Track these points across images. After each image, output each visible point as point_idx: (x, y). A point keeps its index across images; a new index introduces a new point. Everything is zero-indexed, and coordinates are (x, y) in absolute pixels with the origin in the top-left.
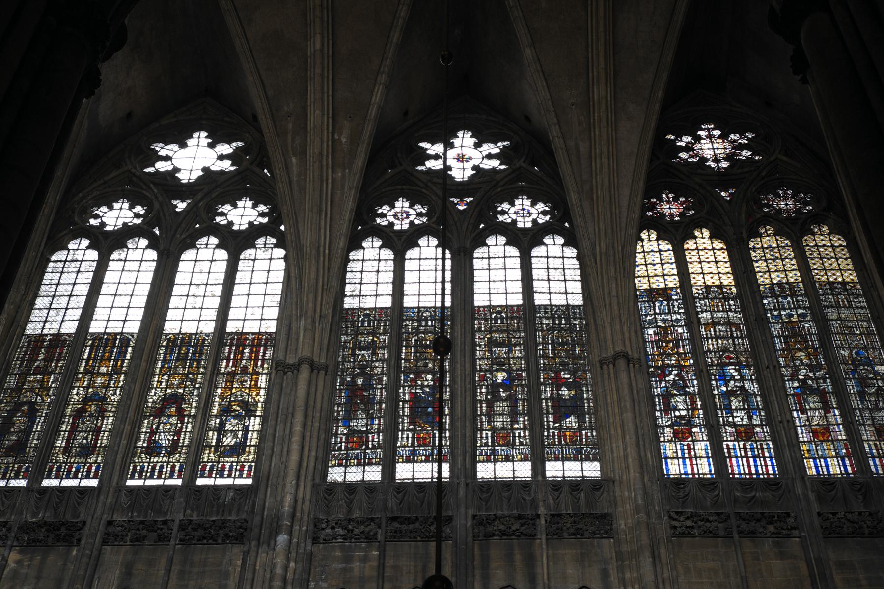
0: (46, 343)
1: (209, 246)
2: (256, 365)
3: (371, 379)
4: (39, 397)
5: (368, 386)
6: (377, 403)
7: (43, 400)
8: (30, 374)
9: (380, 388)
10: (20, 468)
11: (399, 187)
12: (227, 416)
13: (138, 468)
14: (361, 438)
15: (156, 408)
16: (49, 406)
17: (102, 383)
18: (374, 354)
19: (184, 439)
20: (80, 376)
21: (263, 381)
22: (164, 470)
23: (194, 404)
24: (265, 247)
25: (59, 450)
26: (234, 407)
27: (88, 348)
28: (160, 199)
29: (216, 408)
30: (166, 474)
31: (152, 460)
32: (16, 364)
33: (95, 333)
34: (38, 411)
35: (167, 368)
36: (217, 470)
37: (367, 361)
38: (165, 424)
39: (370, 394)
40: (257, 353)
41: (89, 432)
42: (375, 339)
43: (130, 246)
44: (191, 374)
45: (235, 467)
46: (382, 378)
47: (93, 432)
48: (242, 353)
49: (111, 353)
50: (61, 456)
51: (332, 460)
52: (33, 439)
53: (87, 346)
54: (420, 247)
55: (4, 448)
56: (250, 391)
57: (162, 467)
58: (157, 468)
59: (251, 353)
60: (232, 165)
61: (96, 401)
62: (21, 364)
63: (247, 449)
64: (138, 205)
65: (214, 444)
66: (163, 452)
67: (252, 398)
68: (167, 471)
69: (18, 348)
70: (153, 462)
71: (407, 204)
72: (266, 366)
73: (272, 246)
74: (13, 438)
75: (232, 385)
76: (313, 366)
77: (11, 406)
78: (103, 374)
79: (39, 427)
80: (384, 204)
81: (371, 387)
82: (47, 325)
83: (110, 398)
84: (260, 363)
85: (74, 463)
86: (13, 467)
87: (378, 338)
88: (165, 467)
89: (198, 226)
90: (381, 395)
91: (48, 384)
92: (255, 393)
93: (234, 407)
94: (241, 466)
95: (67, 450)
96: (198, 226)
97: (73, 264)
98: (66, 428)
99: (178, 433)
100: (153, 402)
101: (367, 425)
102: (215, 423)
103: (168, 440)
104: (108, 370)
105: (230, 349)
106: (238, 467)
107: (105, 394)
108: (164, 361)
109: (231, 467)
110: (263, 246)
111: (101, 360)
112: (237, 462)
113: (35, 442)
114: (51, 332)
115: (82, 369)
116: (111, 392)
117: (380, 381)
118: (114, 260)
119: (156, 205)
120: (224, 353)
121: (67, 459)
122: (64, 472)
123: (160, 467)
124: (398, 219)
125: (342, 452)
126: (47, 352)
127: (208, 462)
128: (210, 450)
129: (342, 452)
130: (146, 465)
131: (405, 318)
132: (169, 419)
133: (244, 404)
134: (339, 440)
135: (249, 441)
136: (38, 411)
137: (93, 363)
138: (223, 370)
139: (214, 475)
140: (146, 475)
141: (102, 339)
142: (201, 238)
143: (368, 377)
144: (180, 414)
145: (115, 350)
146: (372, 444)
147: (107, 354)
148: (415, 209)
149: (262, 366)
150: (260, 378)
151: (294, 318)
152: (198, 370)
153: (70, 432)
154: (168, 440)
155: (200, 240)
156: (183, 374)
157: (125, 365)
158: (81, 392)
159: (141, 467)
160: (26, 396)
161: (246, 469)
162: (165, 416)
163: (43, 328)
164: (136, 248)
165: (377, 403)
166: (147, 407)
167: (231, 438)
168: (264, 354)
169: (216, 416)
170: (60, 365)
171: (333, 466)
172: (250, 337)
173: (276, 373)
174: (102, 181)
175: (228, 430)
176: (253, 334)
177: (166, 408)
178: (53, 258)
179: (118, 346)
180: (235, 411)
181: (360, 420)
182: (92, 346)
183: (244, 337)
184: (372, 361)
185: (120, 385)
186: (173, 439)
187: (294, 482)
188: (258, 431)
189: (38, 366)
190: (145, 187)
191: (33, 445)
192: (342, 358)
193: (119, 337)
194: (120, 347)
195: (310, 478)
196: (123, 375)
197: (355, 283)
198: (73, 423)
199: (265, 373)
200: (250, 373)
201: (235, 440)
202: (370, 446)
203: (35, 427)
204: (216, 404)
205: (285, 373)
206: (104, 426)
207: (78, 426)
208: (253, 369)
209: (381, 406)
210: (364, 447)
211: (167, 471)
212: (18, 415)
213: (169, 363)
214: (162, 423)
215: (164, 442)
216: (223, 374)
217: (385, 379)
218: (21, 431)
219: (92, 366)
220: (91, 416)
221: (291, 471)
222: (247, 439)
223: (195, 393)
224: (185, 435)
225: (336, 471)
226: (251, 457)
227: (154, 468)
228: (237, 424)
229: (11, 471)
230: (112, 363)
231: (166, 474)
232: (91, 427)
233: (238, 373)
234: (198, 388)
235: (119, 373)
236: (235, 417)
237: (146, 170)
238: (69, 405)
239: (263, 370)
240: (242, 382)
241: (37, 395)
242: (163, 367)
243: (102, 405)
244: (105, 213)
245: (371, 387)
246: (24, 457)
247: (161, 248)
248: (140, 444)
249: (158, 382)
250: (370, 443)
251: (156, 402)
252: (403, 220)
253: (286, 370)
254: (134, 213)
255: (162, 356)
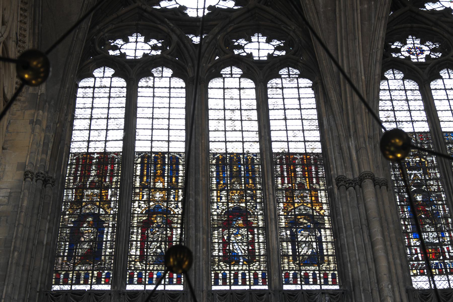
0: (95, 161)
1: (234, 76)
2: (311, 182)
3: (430, 196)
4: (101, 210)
5: (427, 202)
6: (442, 218)
7: (106, 213)
8: (87, 189)
9: (441, 204)
10: (100, 275)
11: (409, 25)
12: (297, 229)
13: (220, 275)
14: (436, 249)
15: (222, 220)
16: (114, 218)
17: (162, 197)
18: (425, 173)
19: (259, 249)
20: (138, 191)
21: (322, 196)
22: (247, 277)
23: (260, 217)
24: (289, 77)
25: (136, 258)
26: (301, 220)
27: (139, 165)
28: (178, 32)
29: (283, 221)
30: (250, 281)
31: (232, 268)
32: (69, 180)
33: (142, 152)
34: (104, 222)
35: (224, 184)
36: (301, 278)
37: (420, 180)
38: (236, 235)
39: (433, 210)
40: (310, 171)
41: (161, 241)
42: (423, 160)
43: (155, 75)
44: (249, 190)
45: (318, 275)
46: (441, 195)
47: (165, 242)
48: (295, 171)
49: (164, 170)
50: (138, 263)
51: (412, 270)
52: (106, 248)
53: (137, 164)
54: (443, 79)
55: (78, 256)
56: (312, 206)
57: (244, 275)
58: (240, 275)
59: (303, 171)
60: (236, 5)
61: (160, 213)
62: (75, 179)
63: (326, 258)
64: (153, 38)
65: (291, 253)
66: (242, 260)
67: (317, 212)
68: (250, 278)
69: (68, 165)
70: (234, 270)
71: (418, 42)
72: (321, 183)
73: (297, 76)
74: (85, 246)
75: (293, 200)
76: (376, 182)
77: (75, 218)
78: (160, 190)
79: (109, 237)
80: (395, 41)
81: (431, 203)
82: (91, 144)
83: (174, 211)
84: (314, 180)
85: (153, 270)
86: (93, 273)
87: (425, 159)
88: (247, 274)
89: (217, 58)
90: (444, 210)
91: (107, 198)
92: (318, 208)
93: (301, 220)
94: (324, 274)
95: (143, 258)
96: (217, 58)
97: (102, 90)
98: (137, 238)
99: (251, 243)
100: (218, 215)
101: (438, 237)
102: (286, 234)
103: (243, 249)
104: (164, 186)
105: (282, 168)
106: (322, 275)
107: (167, 207)
108: (218, 177)
109: (314, 274)
110: (287, 76)
111: (155, 176)
112: (319, 270)
113: (109, 250)
114: (97, 151)
115: (138, 185)
116: (173, 205)
117: (440, 199)
118: (142, 87)
119: (175, 38)
120: (277, 171)
121: (146, 267)
122: (145, 278)
123: (242, 274)
124: (413, 54)
125: (421, 262)
126: (98, 169)
127: (290, 271)
128: (289, 259)
129: (421, 262)
130: (227, 272)
131: (447, 141)
132: (238, 230)
133: (310, 217)
134: (414, 251)
135: (325, 251)
136: (104, 222)
137: (147, 179)
138: (280, 186)
139: (299, 282)
140: (230, 282)
141: (149, 157)
142: (224, 68)
143: (427, 194)
144: (249, 227)
145: (166, 168)
146: (449, 255)
147: (159, 171)
148: (428, 46)
149: (318, 183)
150: (319, 194)
151: (342, 139)
152: (255, 186)
153: (142, 242)
154: (243, 249)
155: (223, 70)
156: (241, 190)
157: (180, 181)
158: (143, 205)
159: (222, 274)
160: (88, 209)
161: (330, 276)
162: (233, 227)
163: (88, 147)
164: (162, 77)
165: (442, 218)
166: (213, 220)
167: (307, 248)
168: (317, 173)
169: (285, 228)
170: (114, 180)
171: (415, 275)
172: (299, 157)
173: (338, 189)
174: (115, 16)
175: (301, 241)
176: (300, 154)
177: (233, 221)
178: (81, 84)
179: (168, 164)
180: (302, 223)
181: (430, 234)
182: (142, 163)
183: (291, 157)
184: (426, 180)
185: (180, 200)
186: (248, 249)
187: (390, 286)
188: (331, 242)
189: (92, 182)
190: (159, 22)
191: (107, 253)
192: (395, 177)
193: (166, 156)
194: (170, 164)
195: (401, 284)
196: (180, 190)
197: (388, 110)
198: (142, 234)
199: (323, 190)
200: (308, 190)
201: (311, 250)
202: (448, 257)
203: (105, 236)
204: (283, 217)
205: (347, 188)
206: (174, 236)
207: (148, 237)
208: (310, 186)
209: (447, 220)
210: (441, 258)
211: (250, 278)
212: (85, 225)
213: (224, 180)
214: (233, 234)
215: (239, 251)
216: (281, 190)
217: (443, 196)
218: (91, 240)
219: (147, 182)
220: (159, 227)
221: (385, 276)
222: (323, 249)
223: (258, 207)
224: (259, 245)
225: (420, 280)
226: (332, 266)
227: (236, 276)
228: (309, 235)
229: (92, 277)
230: (166, 179)
231: (250, 281)
232: (161, 237)
233: (295, 190)
234: (260, 203)
235: (176, 188)
236: (305, 229)
237: (154, 7)
238: (134, 217)
239: (319, 186)
240: (302, 197)
241: (99, 207)
242: (218, 183)
243: (167, 217)
244: (122, 45)
245: (431, 203)
246: (101, 264)
247: (191, 74)
248: (216, 253)
249: (217, 197)
250: (447, 254)
251: (221, 215)
252: (418, 55)
253: (347, 185)
254: (150, 46)
255: (215, 174)
